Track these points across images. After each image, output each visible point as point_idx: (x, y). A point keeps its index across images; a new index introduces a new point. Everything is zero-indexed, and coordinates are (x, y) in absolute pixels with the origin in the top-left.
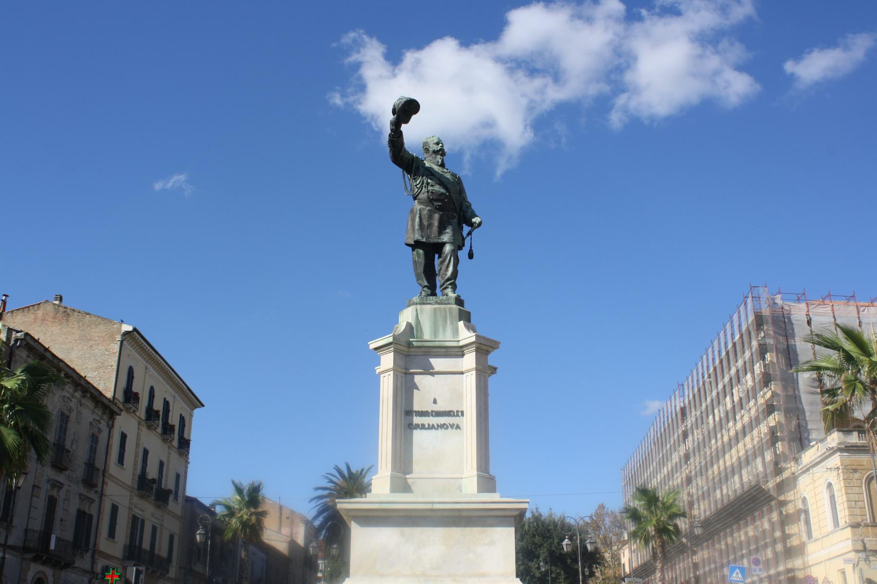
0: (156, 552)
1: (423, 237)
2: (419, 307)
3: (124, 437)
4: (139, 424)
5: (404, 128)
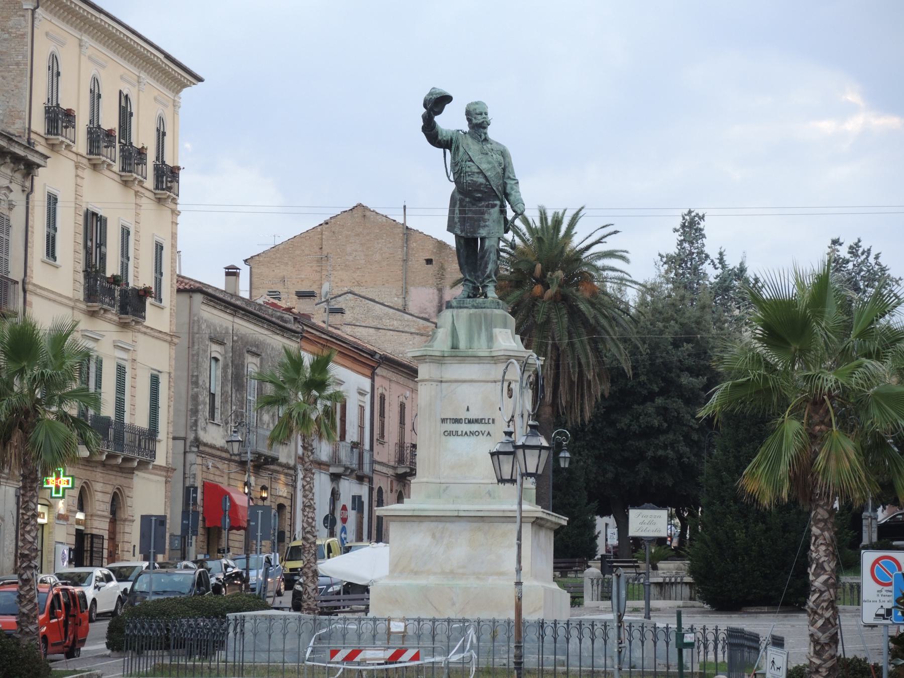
0: (127, 420)
1: (462, 232)
2: (455, 311)
3: (52, 200)
5: (437, 119)
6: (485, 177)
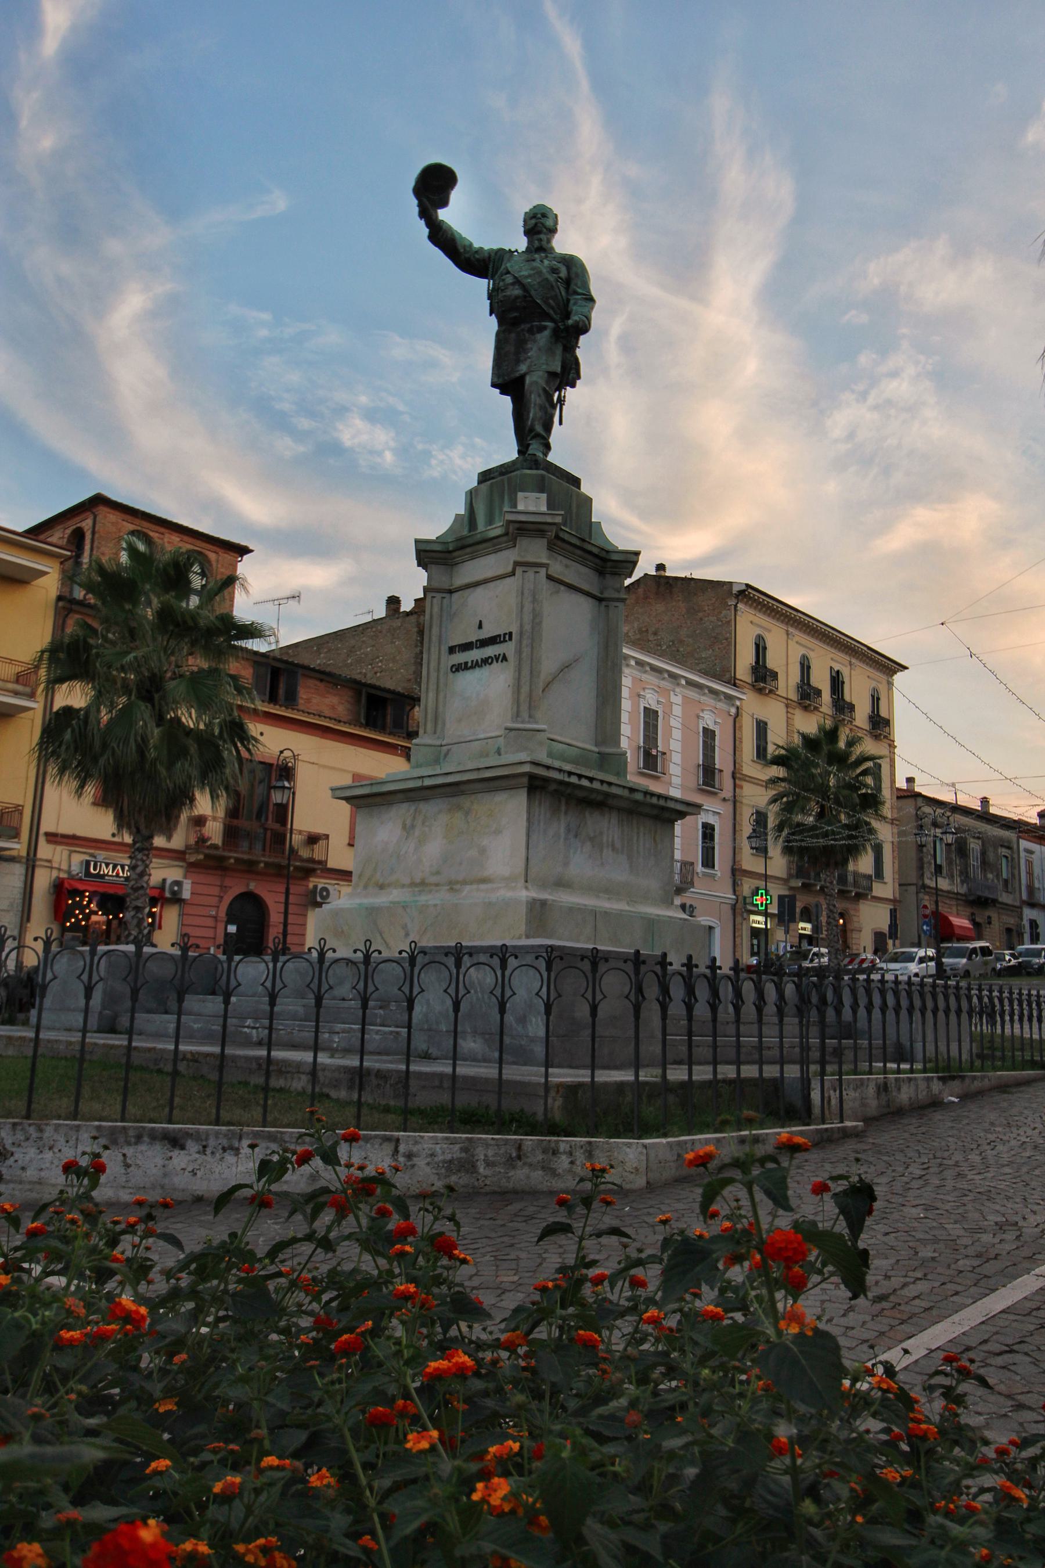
4: (787, 706)
5: (443, 214)
6: (523, 286)
